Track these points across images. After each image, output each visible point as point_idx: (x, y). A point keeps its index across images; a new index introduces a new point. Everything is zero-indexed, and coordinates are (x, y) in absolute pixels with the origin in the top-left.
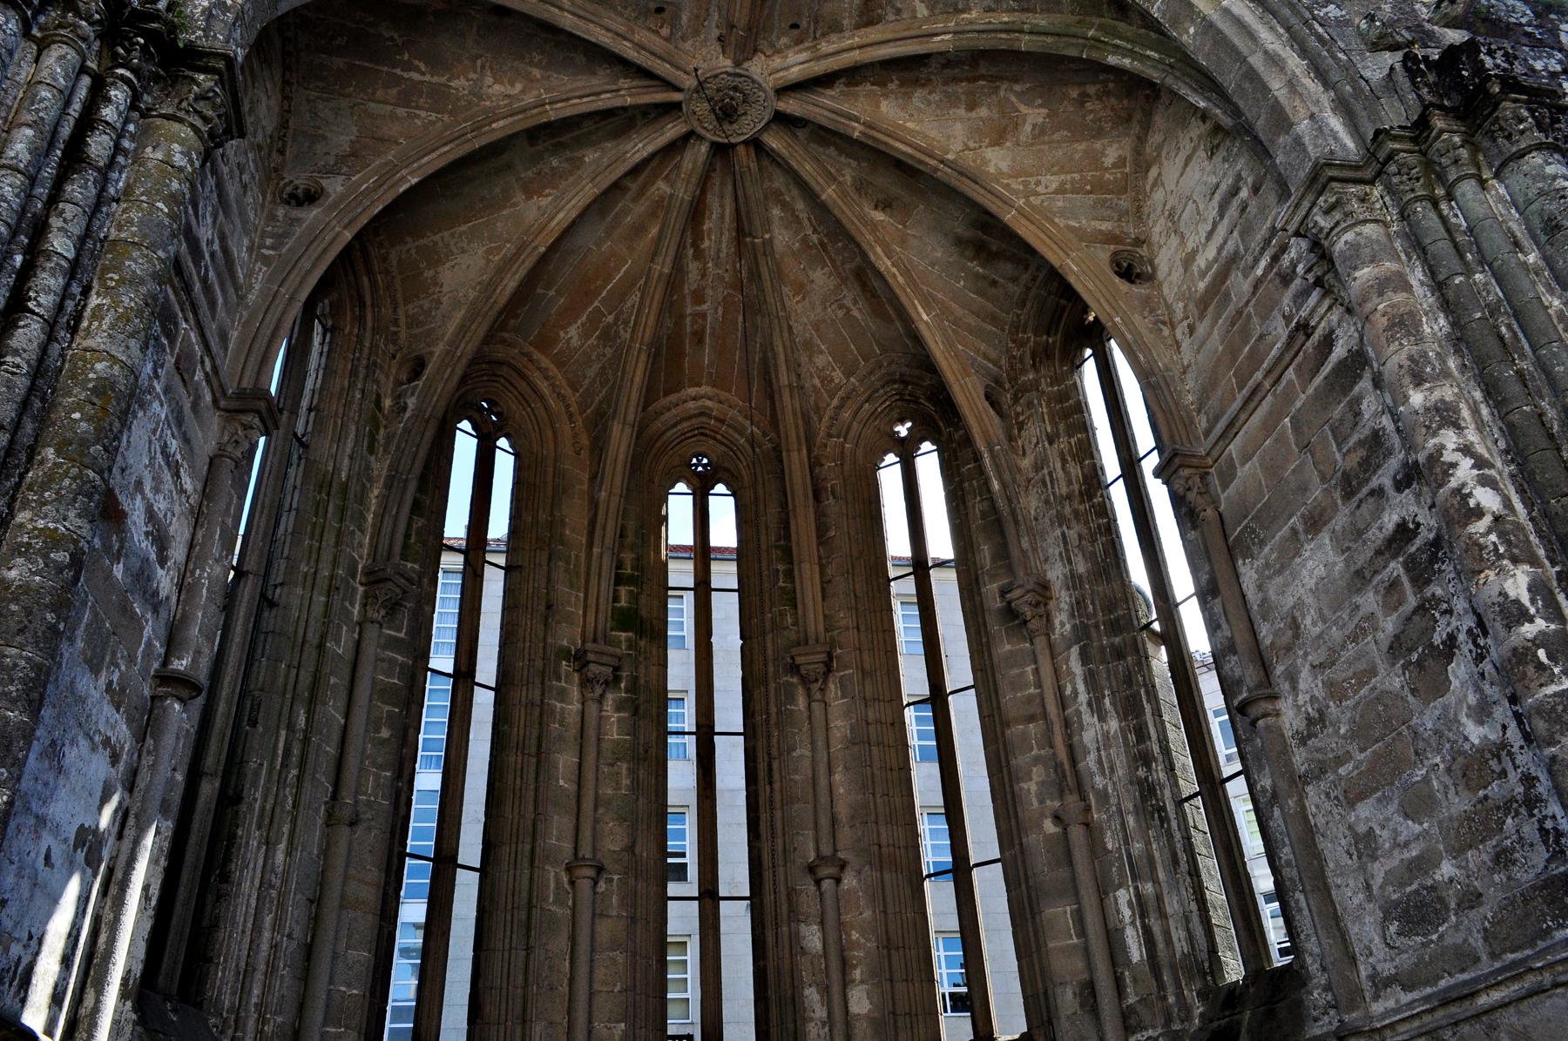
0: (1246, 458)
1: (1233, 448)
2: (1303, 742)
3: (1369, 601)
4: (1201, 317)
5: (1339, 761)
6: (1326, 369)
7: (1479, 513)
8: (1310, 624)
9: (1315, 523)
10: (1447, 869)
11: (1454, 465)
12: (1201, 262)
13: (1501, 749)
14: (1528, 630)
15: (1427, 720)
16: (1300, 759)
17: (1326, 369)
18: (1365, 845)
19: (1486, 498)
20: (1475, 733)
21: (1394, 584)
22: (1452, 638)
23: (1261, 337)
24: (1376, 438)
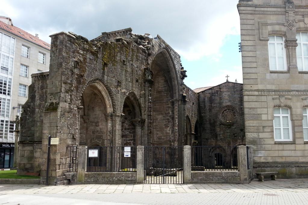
0: (158, 105)
1: (157, 104)
2: (155, 126)
3: (164, 121)
4: (158, 92)
5: (157, 129)
6: (167, 106)
8: (158, 119)
9: (162, 114)
12: (160, 88)
13: (169, 133)
15: (165, 130)
16: (154, 127)
17: (167, 106)
18: (158, 134)
20: (168, 132)
21: (166, 121)
22: (169, 126)
23: (163, 99)
24: (169, 113)
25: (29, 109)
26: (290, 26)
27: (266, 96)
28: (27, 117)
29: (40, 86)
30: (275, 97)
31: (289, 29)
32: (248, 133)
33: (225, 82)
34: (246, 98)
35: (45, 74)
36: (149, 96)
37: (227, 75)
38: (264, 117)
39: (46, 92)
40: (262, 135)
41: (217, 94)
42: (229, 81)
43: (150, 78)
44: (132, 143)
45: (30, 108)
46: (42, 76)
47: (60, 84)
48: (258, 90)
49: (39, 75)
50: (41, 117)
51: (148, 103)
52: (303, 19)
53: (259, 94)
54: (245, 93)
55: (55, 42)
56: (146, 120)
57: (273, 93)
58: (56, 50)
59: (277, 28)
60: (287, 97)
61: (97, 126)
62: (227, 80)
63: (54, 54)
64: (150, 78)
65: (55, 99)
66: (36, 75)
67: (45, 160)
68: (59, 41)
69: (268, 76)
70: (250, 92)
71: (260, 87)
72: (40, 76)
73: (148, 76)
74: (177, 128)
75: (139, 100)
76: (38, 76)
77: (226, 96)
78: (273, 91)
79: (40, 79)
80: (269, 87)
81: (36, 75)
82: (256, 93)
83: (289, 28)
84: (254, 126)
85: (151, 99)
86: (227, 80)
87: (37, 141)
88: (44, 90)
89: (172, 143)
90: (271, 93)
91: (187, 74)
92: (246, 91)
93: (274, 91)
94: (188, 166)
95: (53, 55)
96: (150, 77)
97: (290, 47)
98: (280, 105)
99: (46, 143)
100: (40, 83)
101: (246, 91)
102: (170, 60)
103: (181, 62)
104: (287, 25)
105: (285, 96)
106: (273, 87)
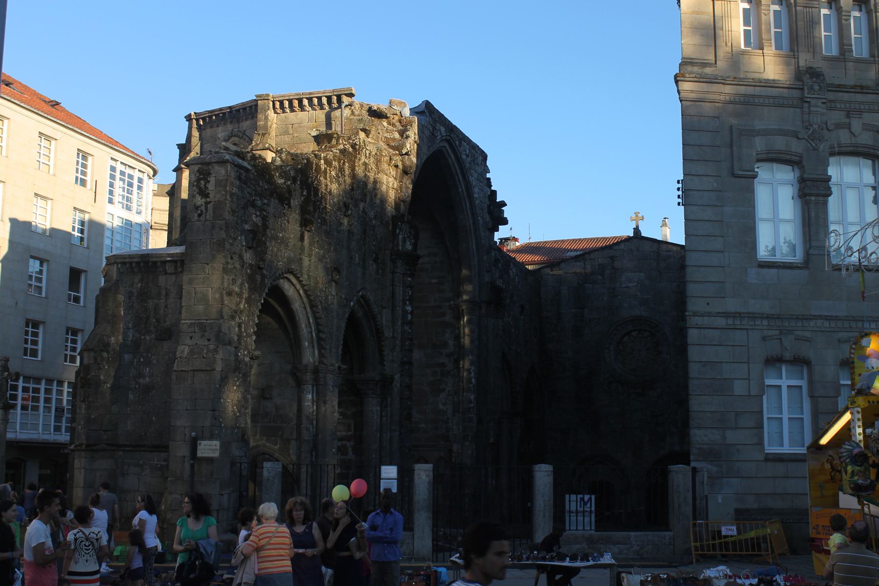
7: (472, 383)
10: (423, 425)
11: (472, 373)
14: (472, 405)
19: (473, 381)
20: (441, 407)
25: (105, 355)
26: (812, 140)
27: (745, 332)
28: (102, 377)
29: (135, 291)
30: (770, 333)
31: (811, 148)
32: (696, 431)
33: (629, 239)
34: (693, 335)
35: (155, 259)
36: (405, 304)
37: (637, 214)
38: (739, 388)
40: (732, 437)
41: (600, 277)
42: (644, 234)
43: (409, 246)
44: (350, 450)
45: (108, 352)
47: (217, 296)
48: (726, 315)
49: (136, 260)
51: (403, 324)
52: (847, 120)
53: (728, 324)
54: (693, 321)
55: (203, 182)
56: (396, 377)
57: (765, 322)
59: (780, 143)
60: (800, 333)
61: (265, 399)
62: (637, 230)
63: (199, 215)
64: (409, 246)
65: (203, 336)
66: (125, 258)
68: (212, 179)
69: (753, 274)
70: (705, 318)
71: (732, 305)
72: (138, 263)
73: (404, 241)
74: (472, 397)
75: (379, 317)
76: (131, 263)
77: (630, 285)
78: (764, 318)
79: (136, 270)
80: (755, 306)
81: (128, 260)
82: (721, 322)
83: (811, 144)
84: (713, 412)
85: (412, 313)
86: (637, 230)
87: (126, 443)
88: (151, 304)
89: (455, 448)
90: (758, 322)
91: (507, 212)
92: (695, 314)
93: (768, 317)
94: (544, 516)
95: (196, 218)
96: (408, 243)
97: (813, 198)
98: (782, 355)
99: (180, 450)
100: (136, 280)
101: (695, 314)
102: (457, 173)
103: (488, 175)
104: (806, 138)
105: (796, 332)
106: (766, 307)
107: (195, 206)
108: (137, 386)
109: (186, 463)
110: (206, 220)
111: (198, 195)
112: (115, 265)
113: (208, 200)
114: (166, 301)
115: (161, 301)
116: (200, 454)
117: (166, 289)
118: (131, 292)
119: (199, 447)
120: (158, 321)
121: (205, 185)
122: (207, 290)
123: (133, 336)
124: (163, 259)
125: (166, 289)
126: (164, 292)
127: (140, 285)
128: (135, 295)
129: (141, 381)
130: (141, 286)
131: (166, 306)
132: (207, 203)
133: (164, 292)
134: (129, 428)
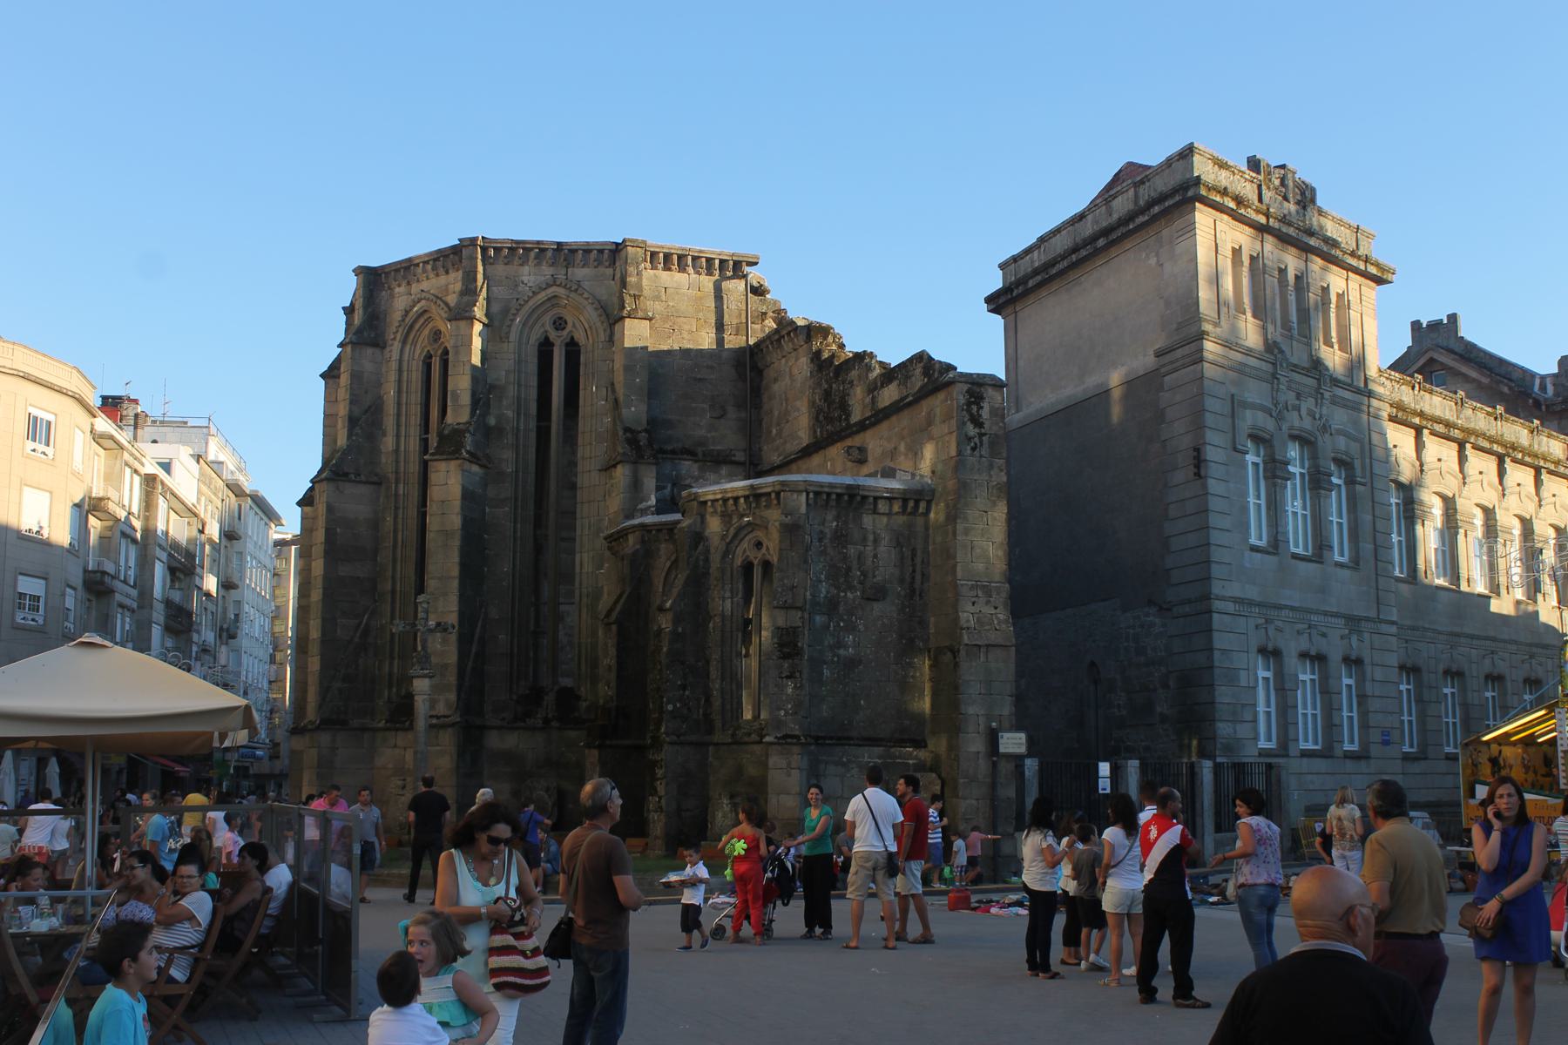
29: (827, 530)
35: (866, 493)
39: (859, 558)
46: (852, 497)
48: (1236, 600)
49: (839, 491)
50: (839, 648)
55: (974, 408)
58: (981, 435)
63: (973, 449)
65: (988, 602)
66: (822, 487)
67: (974, 802)
68: (986, 405)
72: (839, 495)
78: (1255, 605)
88: (852, 551)
95: (969, 452)
100: (829, 517)
107: (966, 436)
108: (836, 659)
109: (980, 761)
110: (981, 456)
111: (969, 423)
112: (804, 494)
113: (983, 431)
114: (875, 549)
115: (867, 548)
116: (1002, 750)
117: (874, 533)
118: (821, 532)
119: (1001, 741)
120: (864, 574)
121: (978, 411)
122: (988, 545)
123: (828, 592)
124: (878, 494)
125: (874, 533)
126: (871, 537)
127: (835, 524)
128: (828, 536)
129: (842, 652)
130: (837, 526)
131: (875, 556)
132: (981, 435)
133: (871, 537)
134: (825, 714)
